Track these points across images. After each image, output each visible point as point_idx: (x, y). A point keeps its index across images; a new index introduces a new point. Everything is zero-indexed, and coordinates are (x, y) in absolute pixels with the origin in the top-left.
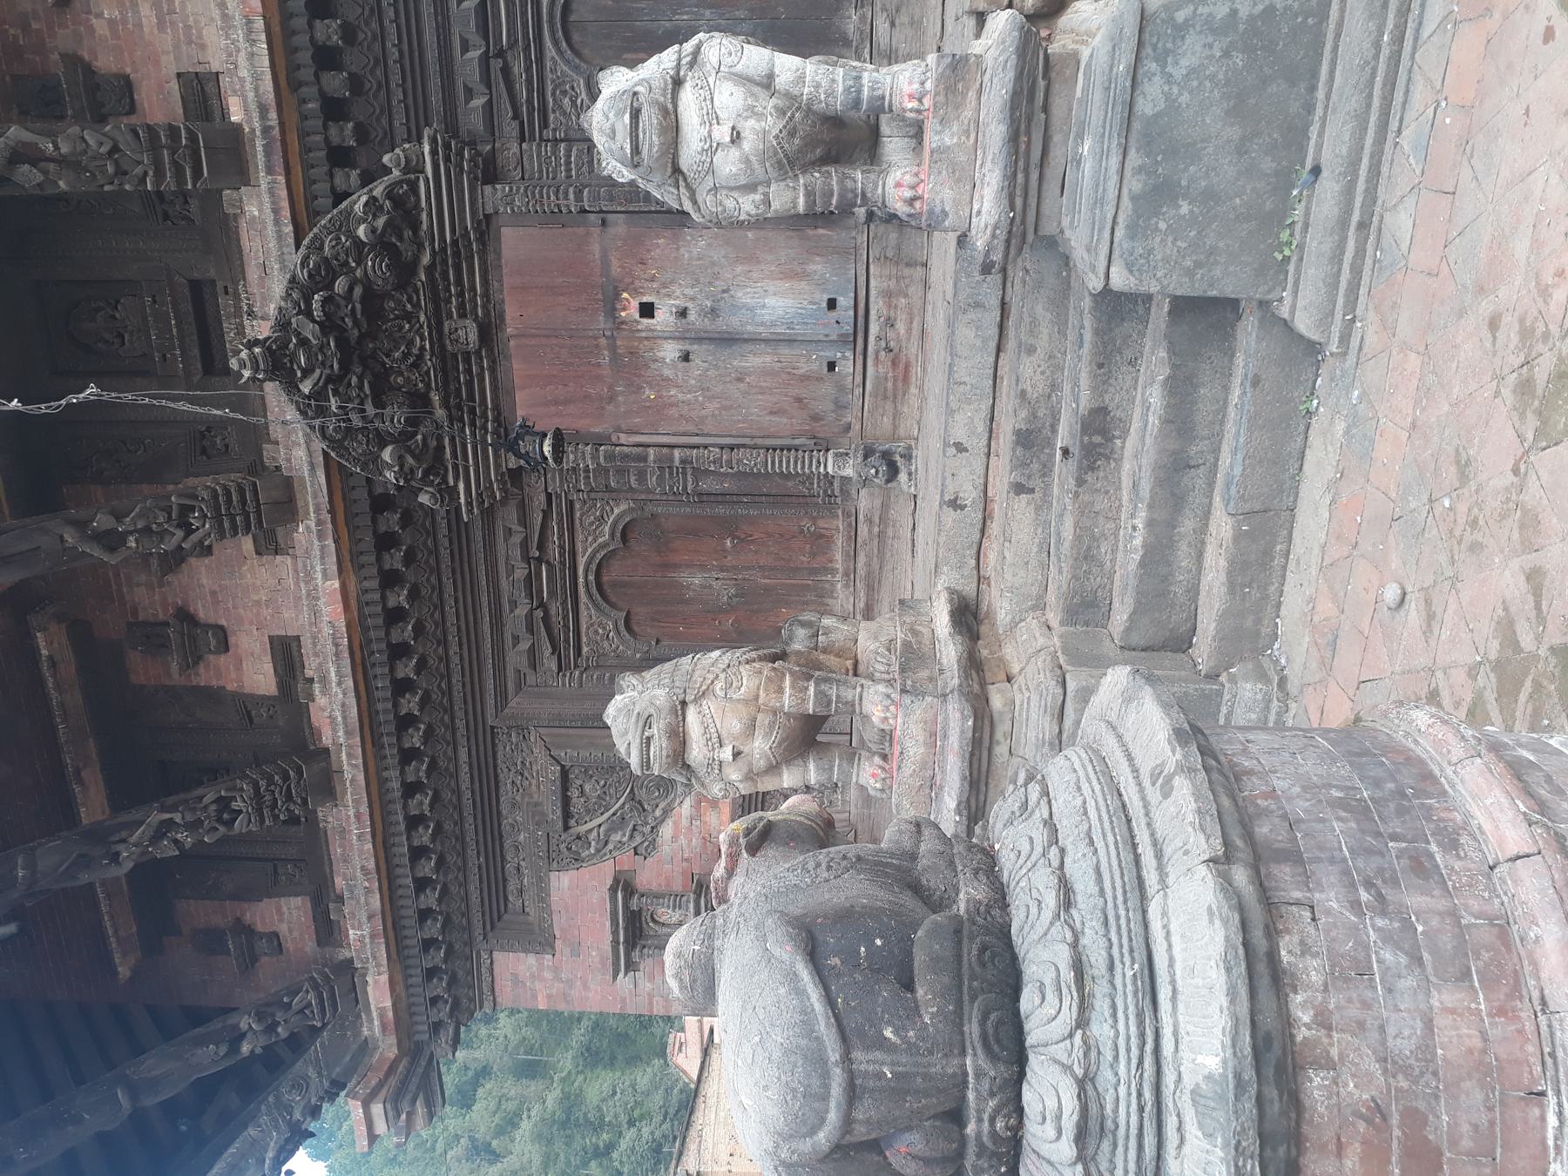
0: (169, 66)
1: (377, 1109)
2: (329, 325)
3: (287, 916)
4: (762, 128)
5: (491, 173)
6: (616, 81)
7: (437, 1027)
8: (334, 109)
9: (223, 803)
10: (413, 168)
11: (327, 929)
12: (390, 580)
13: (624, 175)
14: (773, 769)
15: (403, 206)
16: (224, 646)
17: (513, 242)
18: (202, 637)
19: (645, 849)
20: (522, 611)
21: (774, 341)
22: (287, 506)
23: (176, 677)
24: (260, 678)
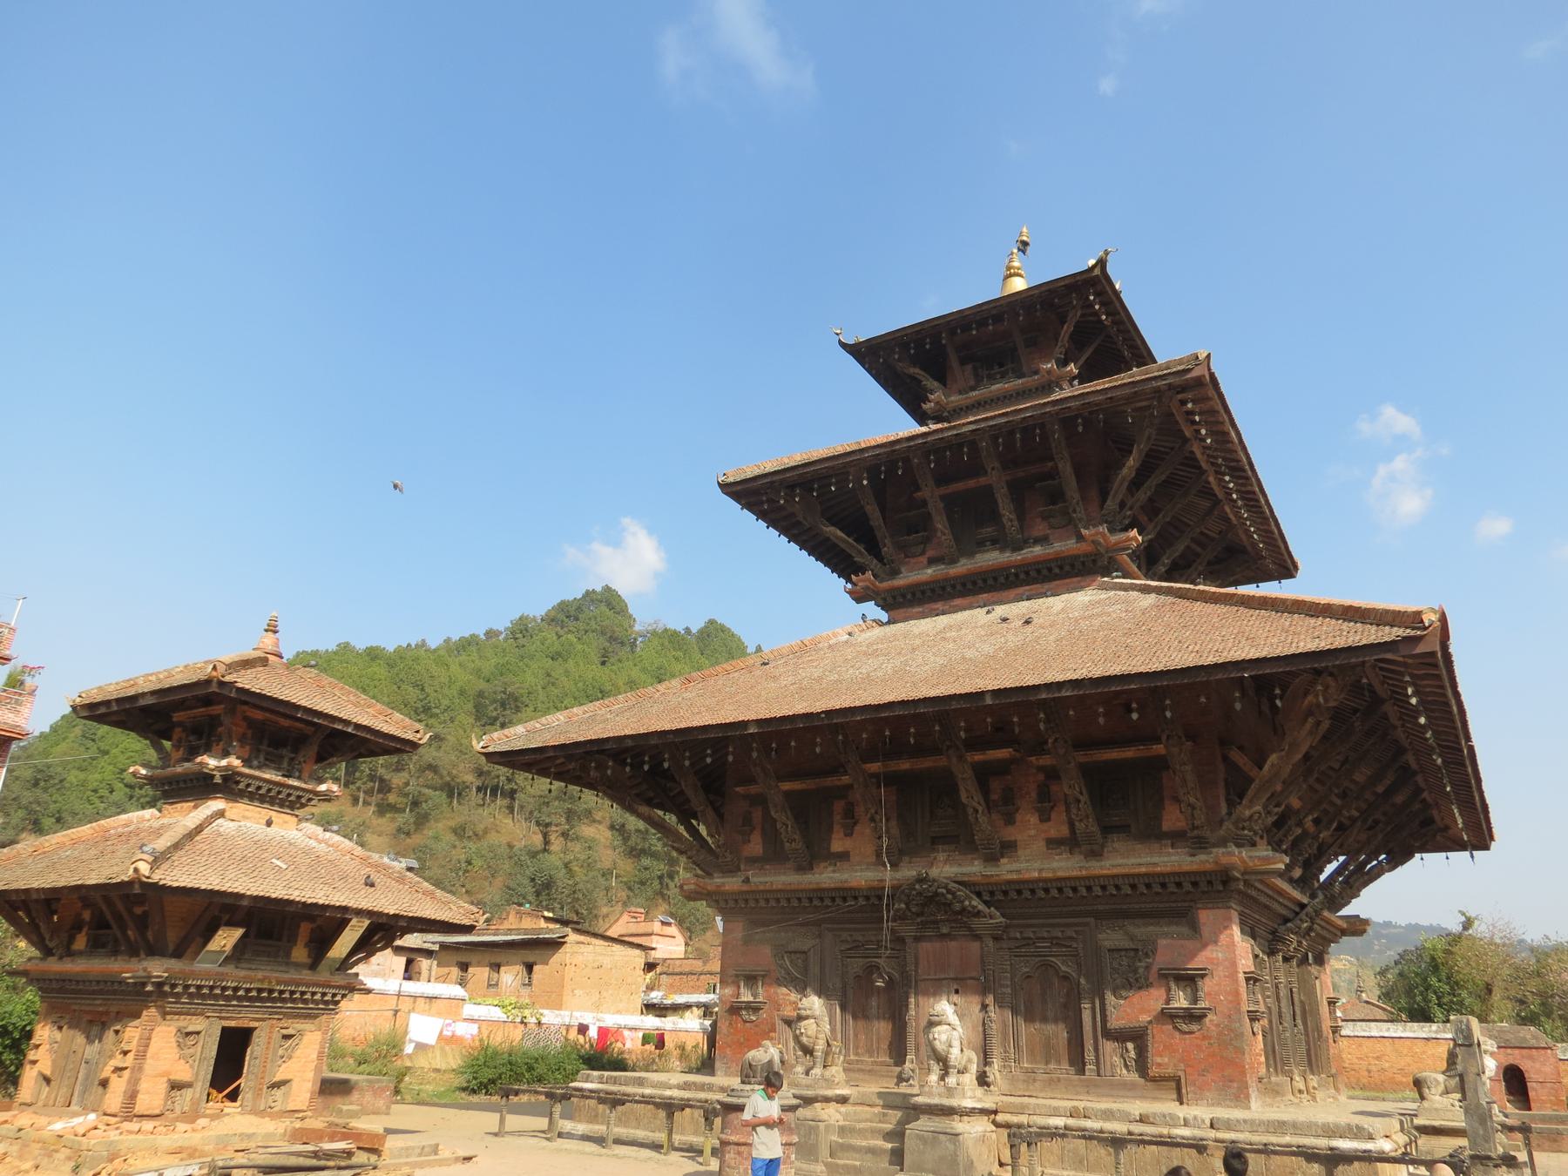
0: (1019, 837)
3: (755, 846)
5: (996, 938)
8: (1005, 893)
11: (753, 861)
12: (867, 898)
17: (976, 945)
23: (837, 818)
24: (837, 845)
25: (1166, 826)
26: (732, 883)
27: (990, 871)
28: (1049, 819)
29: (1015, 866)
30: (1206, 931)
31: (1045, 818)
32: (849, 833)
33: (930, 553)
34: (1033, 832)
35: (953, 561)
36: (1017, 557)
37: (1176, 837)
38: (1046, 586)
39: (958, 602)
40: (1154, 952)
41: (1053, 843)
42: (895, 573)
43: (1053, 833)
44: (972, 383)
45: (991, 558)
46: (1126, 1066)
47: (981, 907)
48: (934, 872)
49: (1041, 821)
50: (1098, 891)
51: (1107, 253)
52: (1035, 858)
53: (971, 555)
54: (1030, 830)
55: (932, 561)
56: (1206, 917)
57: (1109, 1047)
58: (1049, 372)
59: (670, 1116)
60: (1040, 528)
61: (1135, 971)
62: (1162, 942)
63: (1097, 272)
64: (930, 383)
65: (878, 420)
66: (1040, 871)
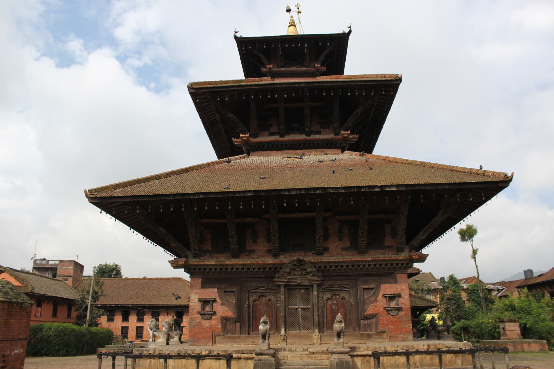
3: (208, 247)
11: (206, 252)
18: (255, 242)
22: (276, 255)
28: (342, 240)
31: (340, 239)
35: (282, 136)
37: (390, 247)
41: (343, 249)
42: (256, 136)
44: (282, 65)
53: (288, 134)
54: (334, 245)
55: (271, 134)
56: (398, 276)
59: (166, 362)
60: (317, 127)
65: (232, 70)
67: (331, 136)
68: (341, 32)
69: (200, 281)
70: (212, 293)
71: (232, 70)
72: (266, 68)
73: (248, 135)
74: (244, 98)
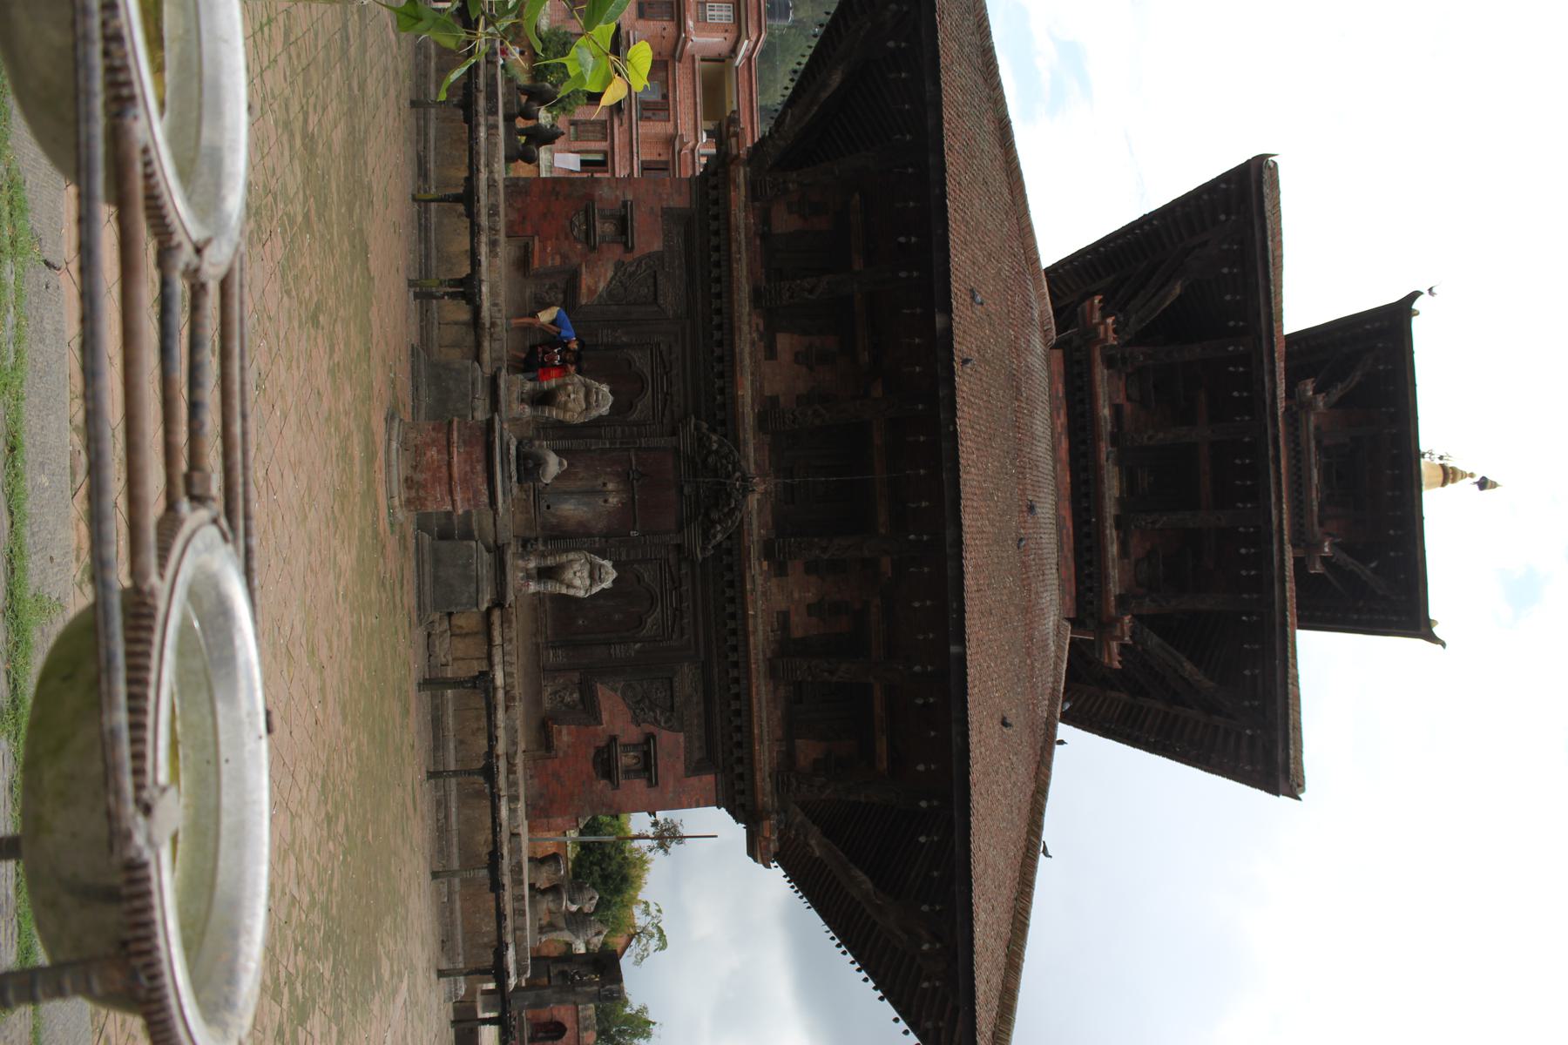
1: (734, 152)
2: (729, 496)
3: (785, 222)
4: (569, 575)
5: (679, 547)
6: (607, 584)
7: (715, 174)
8: (730, 568)
9: (791, 297)
10: (704, 549)
11: (765, 219)
12: (722, 391)
13: (605, 562)
14: (558, 387)
15: (706, 536)
16: (797, 354)
19: (619, 265)
20: (674, 372)
21: (572, 493)
22: (762, 421)
24: (784, 341)
25: (799, 742)
26: (739, 196)
27: (754, 552)
29: (759, 580)
30: (694, 781)
32: (797, 358)
33: (1128, 408)
34: (796, 595)
35: (1115, 439)
36: (1110, 522)
38: (1070, 555)
39: (1064, 444)
40: (671, 729)
41: (784, 618)
43: (795, 619)
45: (1112, 486)
46: (555, 693)
47: (714, 542)
48: (753, 501)
49: (809, 606)
50: (734, 673)
51: (1443, 644)
52: (770, 599)
53: (1119, 462)
55: (1117, 410)
56: (708, 780)
57: (576, 677)
58: (1320, 546)
61: (651, 709)
62: (681, 737)
63: (1423, 630)
64: (1337, 392)
66: (755, 616)
67: (1114, 589)
68: (1432, 616)
69: (680, 201)
70: (649, 239)
71: (1311, 296)
72: (1316, 391)
73: (1112, 340)
74: (1231, 324)
